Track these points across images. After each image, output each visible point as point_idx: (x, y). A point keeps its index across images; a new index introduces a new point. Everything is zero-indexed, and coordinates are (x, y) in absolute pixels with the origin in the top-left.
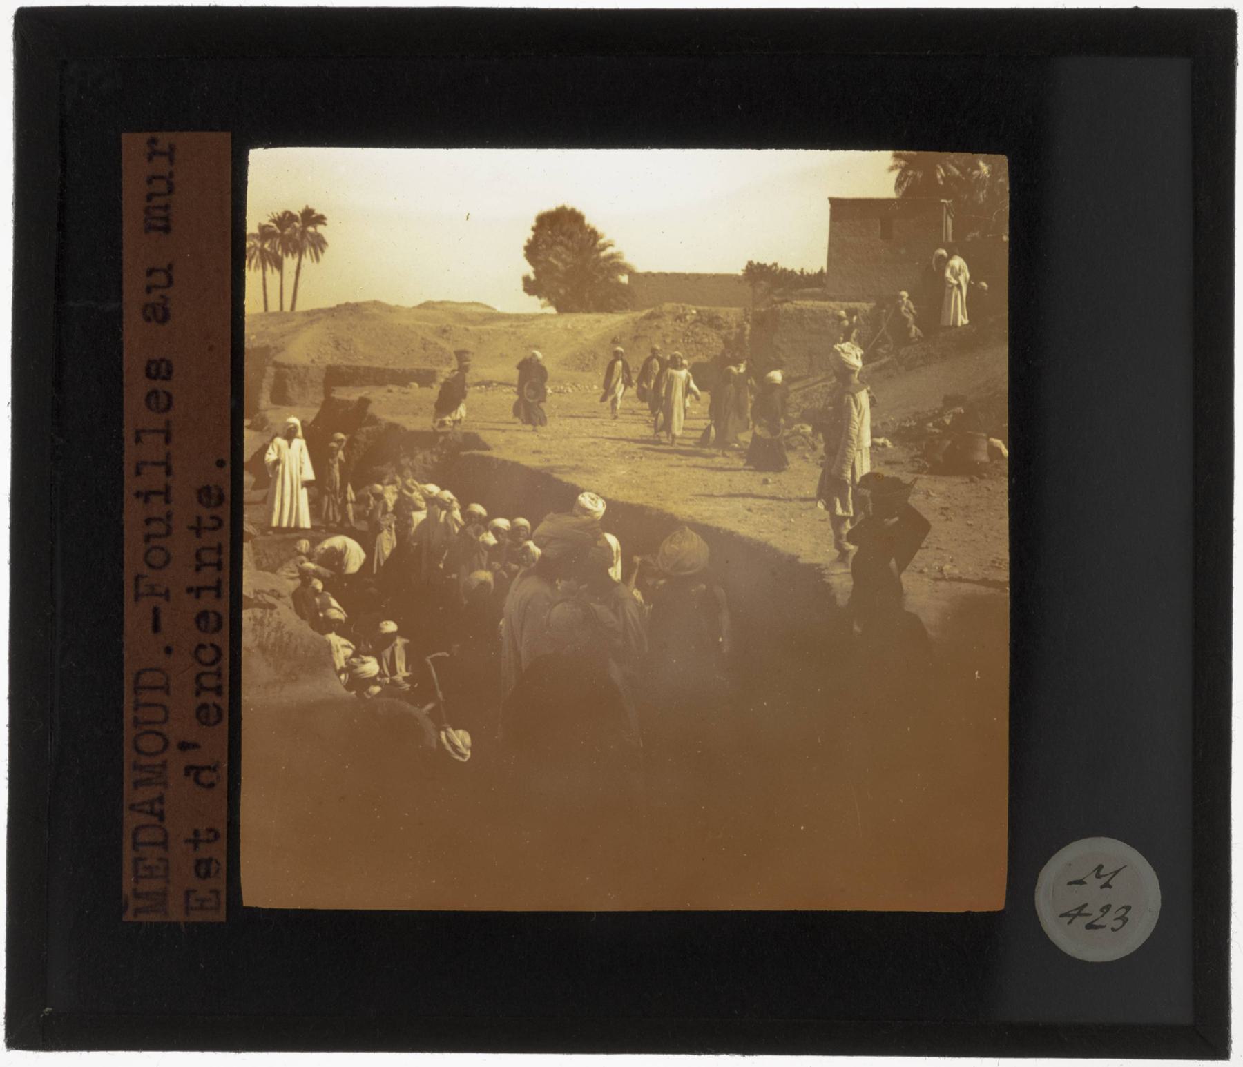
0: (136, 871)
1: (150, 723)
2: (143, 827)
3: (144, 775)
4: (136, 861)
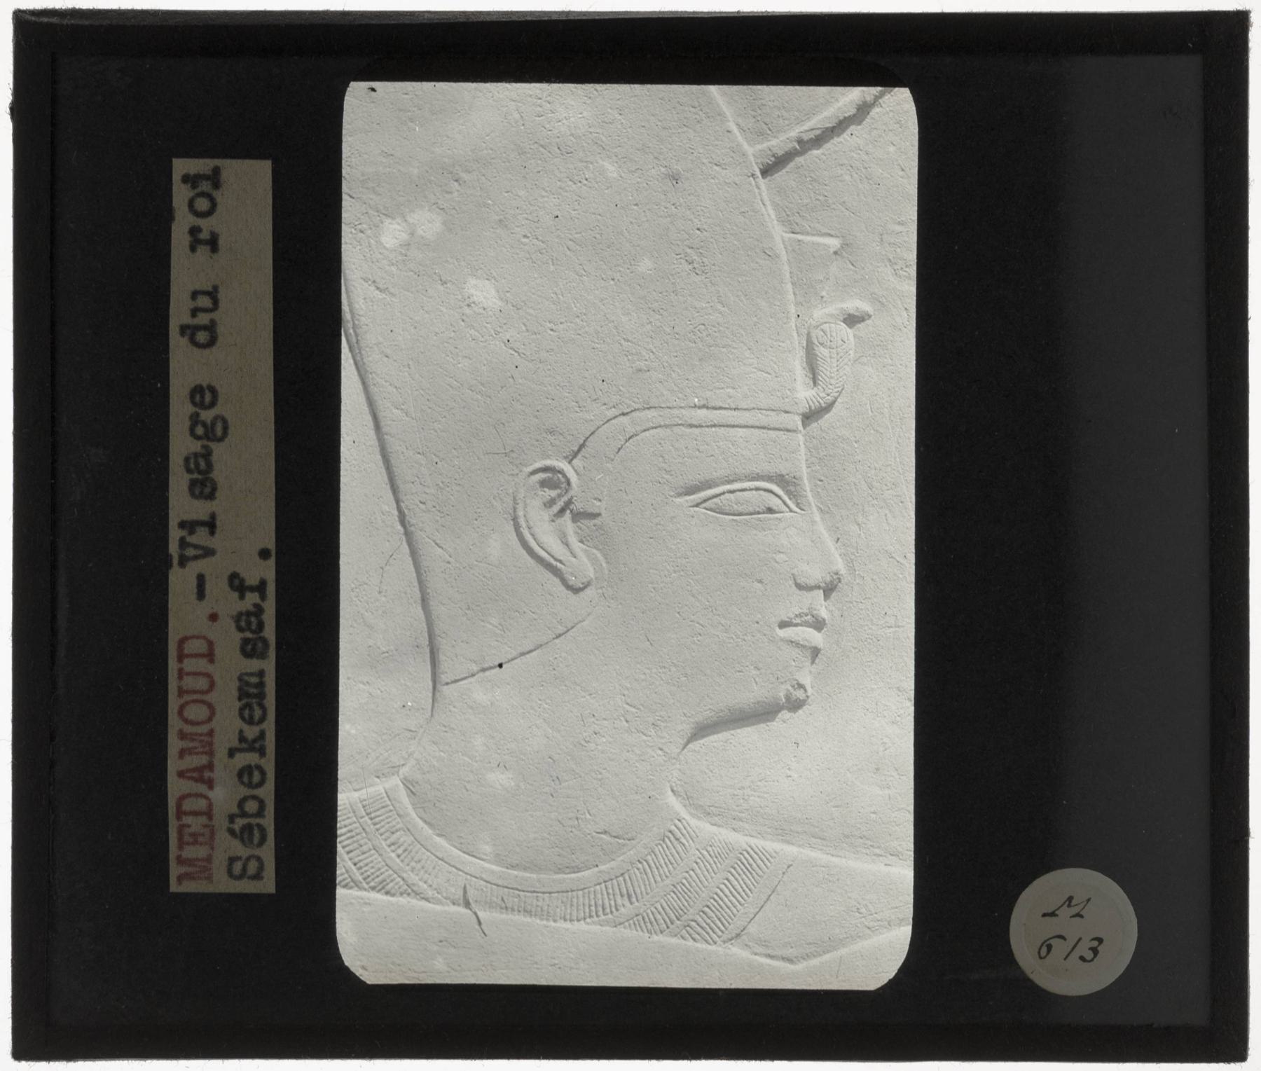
0: (180, 838)
1: (195, 692)
2: (189, 795)
3: (191, 745)
4: (181, 829)
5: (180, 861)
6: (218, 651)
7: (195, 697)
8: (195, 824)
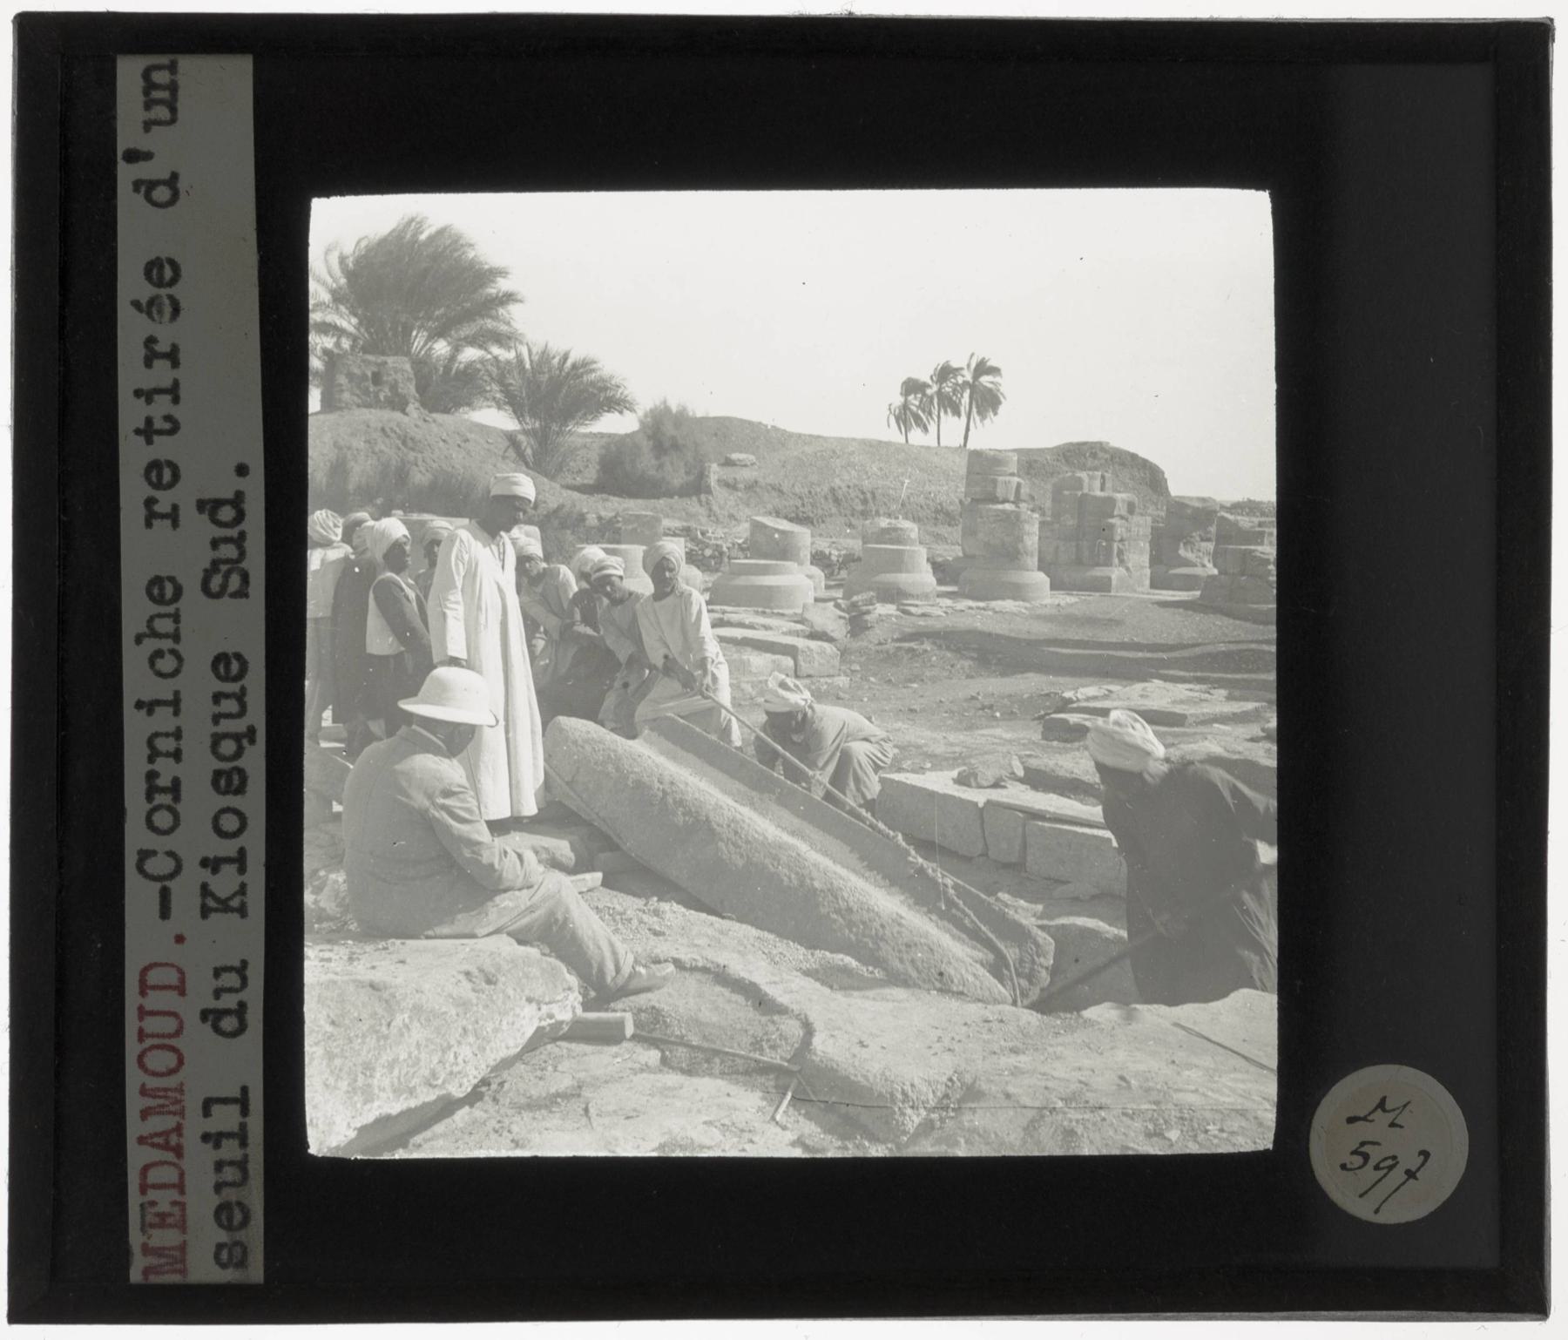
0: (143, 1217)
1: (158, 1036)
5: (146, 1249)
6: (189, 985)
7: (156, 1041)
8: (164, 1200)
